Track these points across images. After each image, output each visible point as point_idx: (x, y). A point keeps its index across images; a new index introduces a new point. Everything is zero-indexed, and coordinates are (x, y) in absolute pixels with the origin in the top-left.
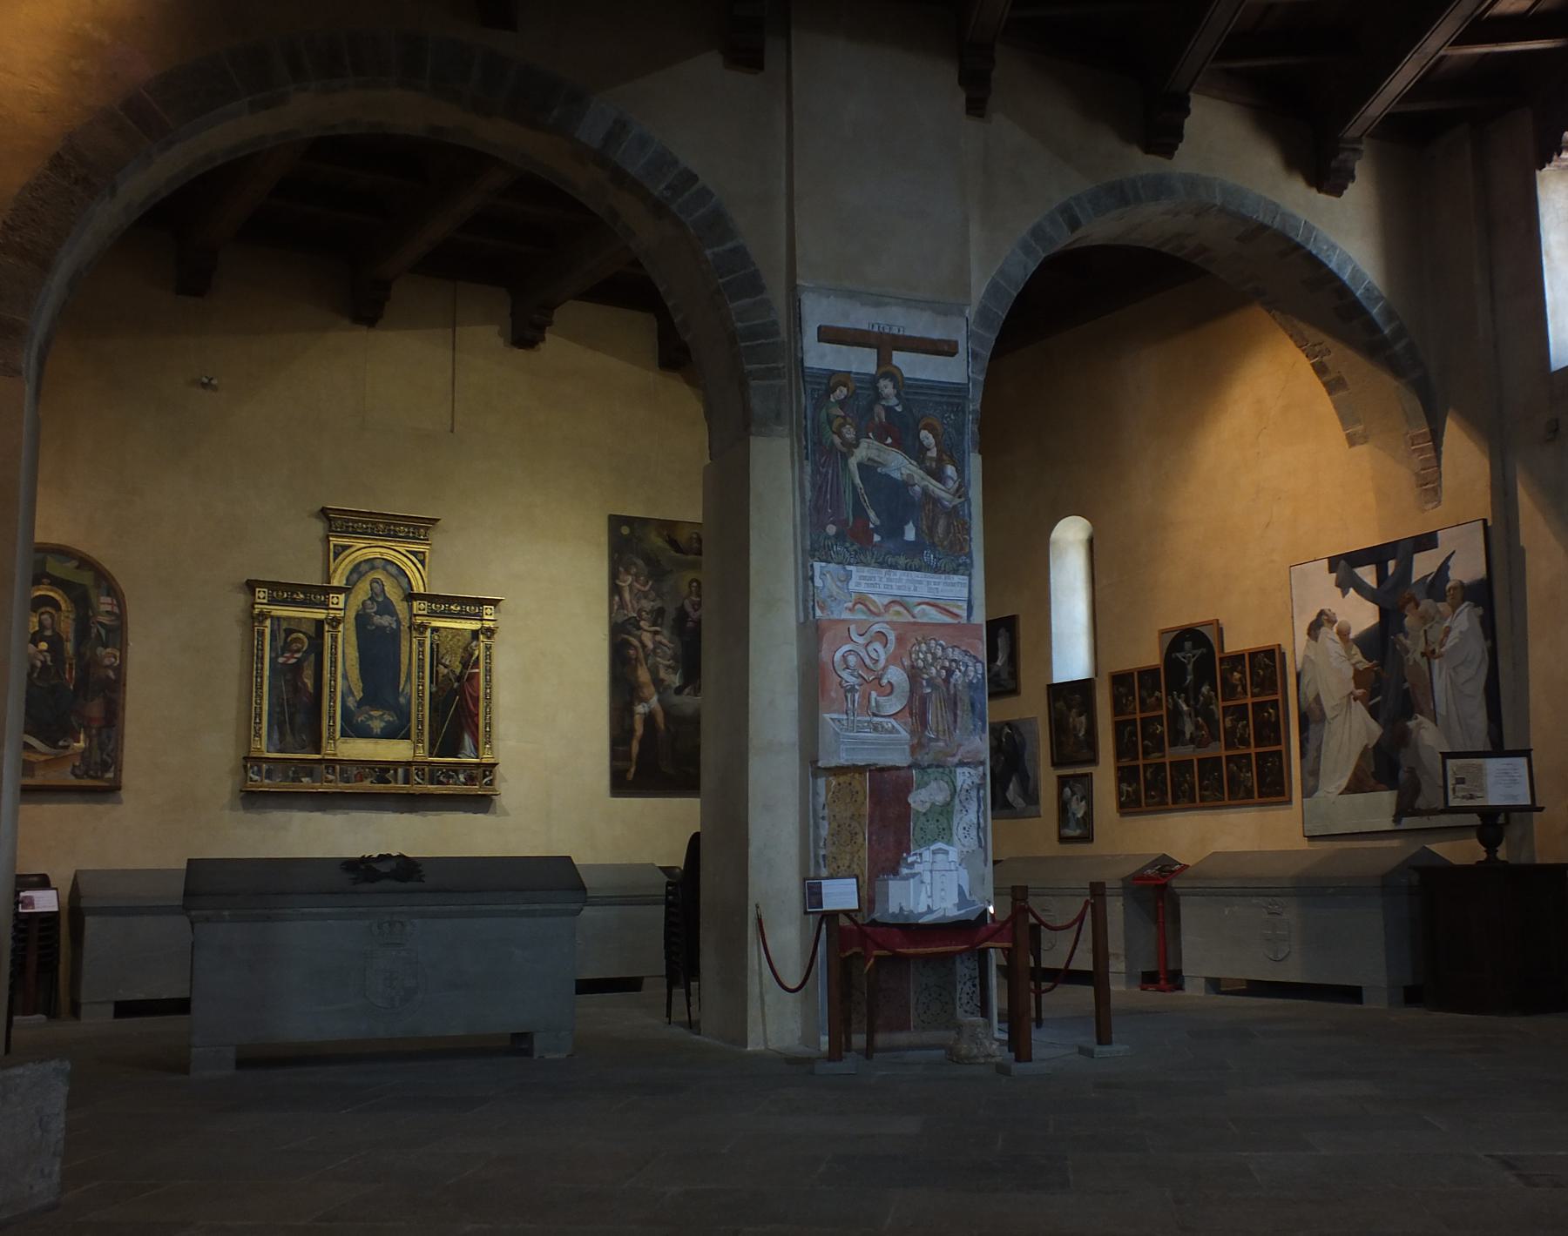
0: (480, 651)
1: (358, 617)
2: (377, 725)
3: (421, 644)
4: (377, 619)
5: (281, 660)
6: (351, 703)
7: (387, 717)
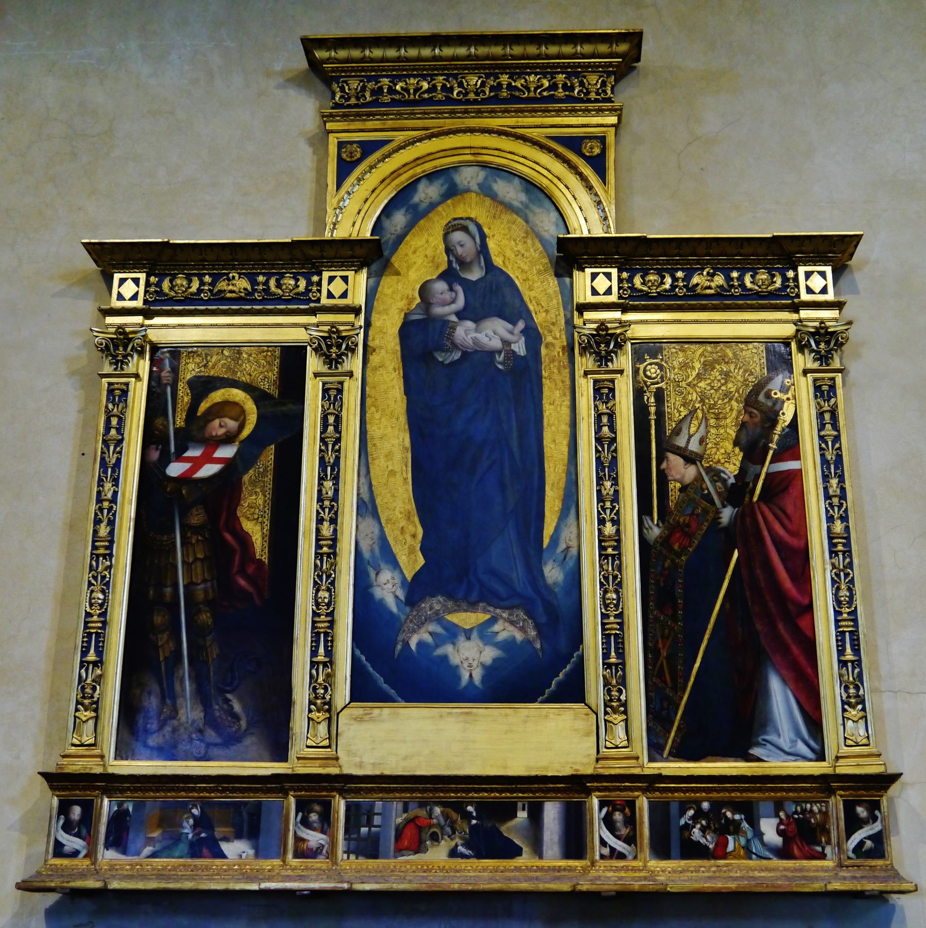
0: (797, 401)
1: (407, 330)
2: (471, 658)
3: (604, 393)
4: (466, 333)
5: (175, 469)
6: (388, 589)
7: (504, 631)
